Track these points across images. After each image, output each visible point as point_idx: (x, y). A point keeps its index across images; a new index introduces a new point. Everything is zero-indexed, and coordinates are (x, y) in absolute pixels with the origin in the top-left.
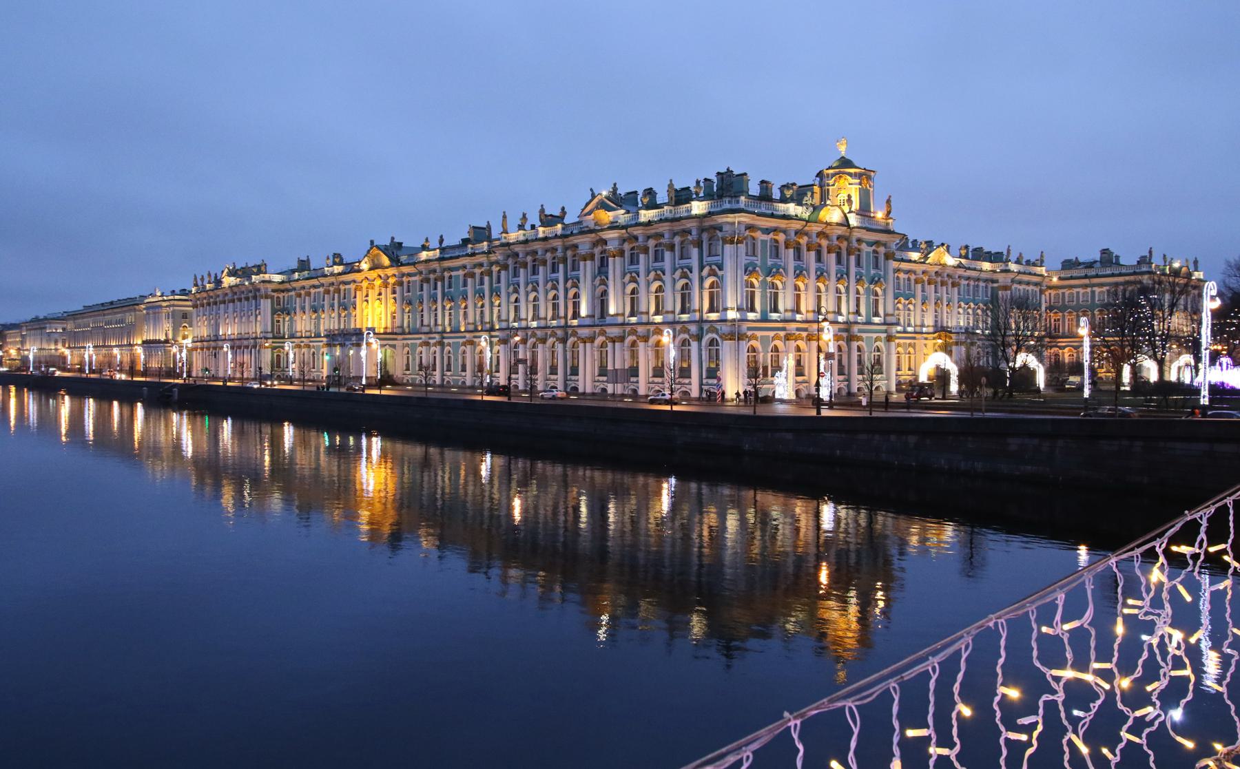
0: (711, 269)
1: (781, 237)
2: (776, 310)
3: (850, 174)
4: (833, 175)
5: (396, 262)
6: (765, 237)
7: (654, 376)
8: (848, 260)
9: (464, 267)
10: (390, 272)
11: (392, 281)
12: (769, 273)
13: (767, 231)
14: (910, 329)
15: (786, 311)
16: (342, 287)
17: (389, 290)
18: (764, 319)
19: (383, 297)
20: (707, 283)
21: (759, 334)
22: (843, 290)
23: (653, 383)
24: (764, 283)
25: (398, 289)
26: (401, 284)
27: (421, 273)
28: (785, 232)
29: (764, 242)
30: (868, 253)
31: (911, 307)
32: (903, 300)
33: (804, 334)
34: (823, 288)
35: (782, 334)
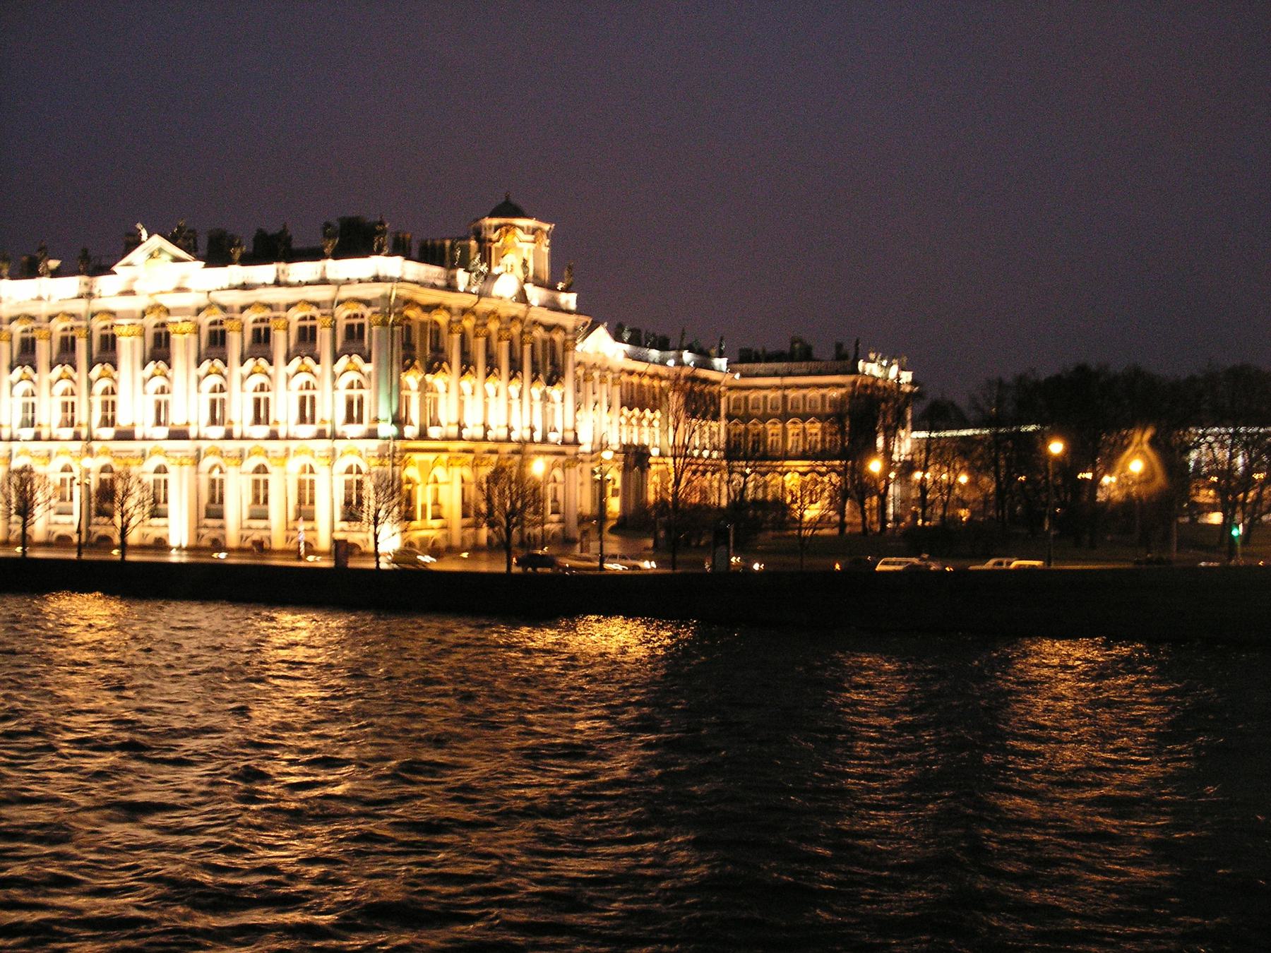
0: (351, 361)
1: (442, 318)
2: (436, 423)
3: (522, 228)
4: (497, 228)
6: (425, 317)
7: (251, 518)
8: (522, 351)
12: (430, 370)
13: (428, 308)
15: (449, 424)
18: (423, 436)
20: (343, 382)
21: (417, 457)
22: (515, 394)
23: (250, 528)
24: (424, 387)
28: (448, 309)
29: (423, 324)
30: (544, 342)
33: (470, 457)
34: (491, 393)
35: (444, 456)
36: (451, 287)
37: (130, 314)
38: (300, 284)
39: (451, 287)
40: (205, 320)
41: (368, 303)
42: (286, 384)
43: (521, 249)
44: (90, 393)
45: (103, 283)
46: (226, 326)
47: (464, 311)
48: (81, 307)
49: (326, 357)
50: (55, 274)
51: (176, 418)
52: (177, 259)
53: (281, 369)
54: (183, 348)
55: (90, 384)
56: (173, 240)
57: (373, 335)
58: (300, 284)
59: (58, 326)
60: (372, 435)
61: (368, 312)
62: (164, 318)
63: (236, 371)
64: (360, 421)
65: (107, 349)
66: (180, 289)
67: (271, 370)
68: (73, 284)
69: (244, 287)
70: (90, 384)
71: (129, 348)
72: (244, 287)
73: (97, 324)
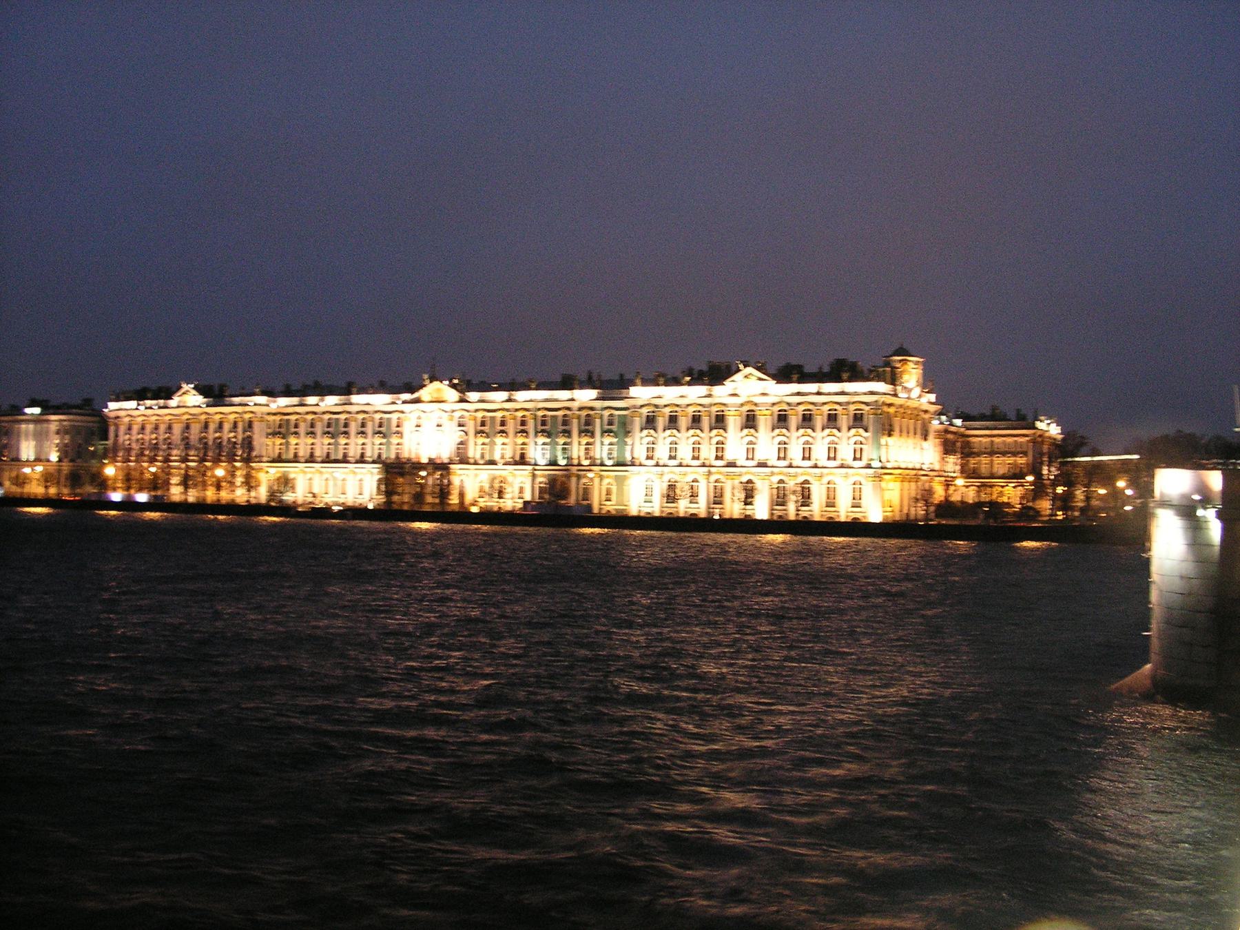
11: (457, 414)
36: (895, 395)
37: (734, 405)
38: (829, 394)
39: (895, 395)
40: (776, 408)
41: (867, 404)
42: (821, 441)
43: (912, 374)
45: (717, 390)
46: (789, 412)
47: (901, 406)
48: (706, 401)
49: (844, 428)
50: (689, 384)
51: (760, 456)
52: (760, 379)
53: (819, 434)
54: (764, 422)
56: (758, 369)
57: (870, 420)
58: (829, 394)
59: (691, 410)
60: (869, 466)
61: (867, 408)
62: (753, 408)
63: (794, 434)
64: (860, 459)
65: (720, 421)
66: (764, 394)
67: (813, 434)
68: (701, 390)
69: (798, 394)
71: (733, 422)
72: (798, 394)
73: (714, 409)
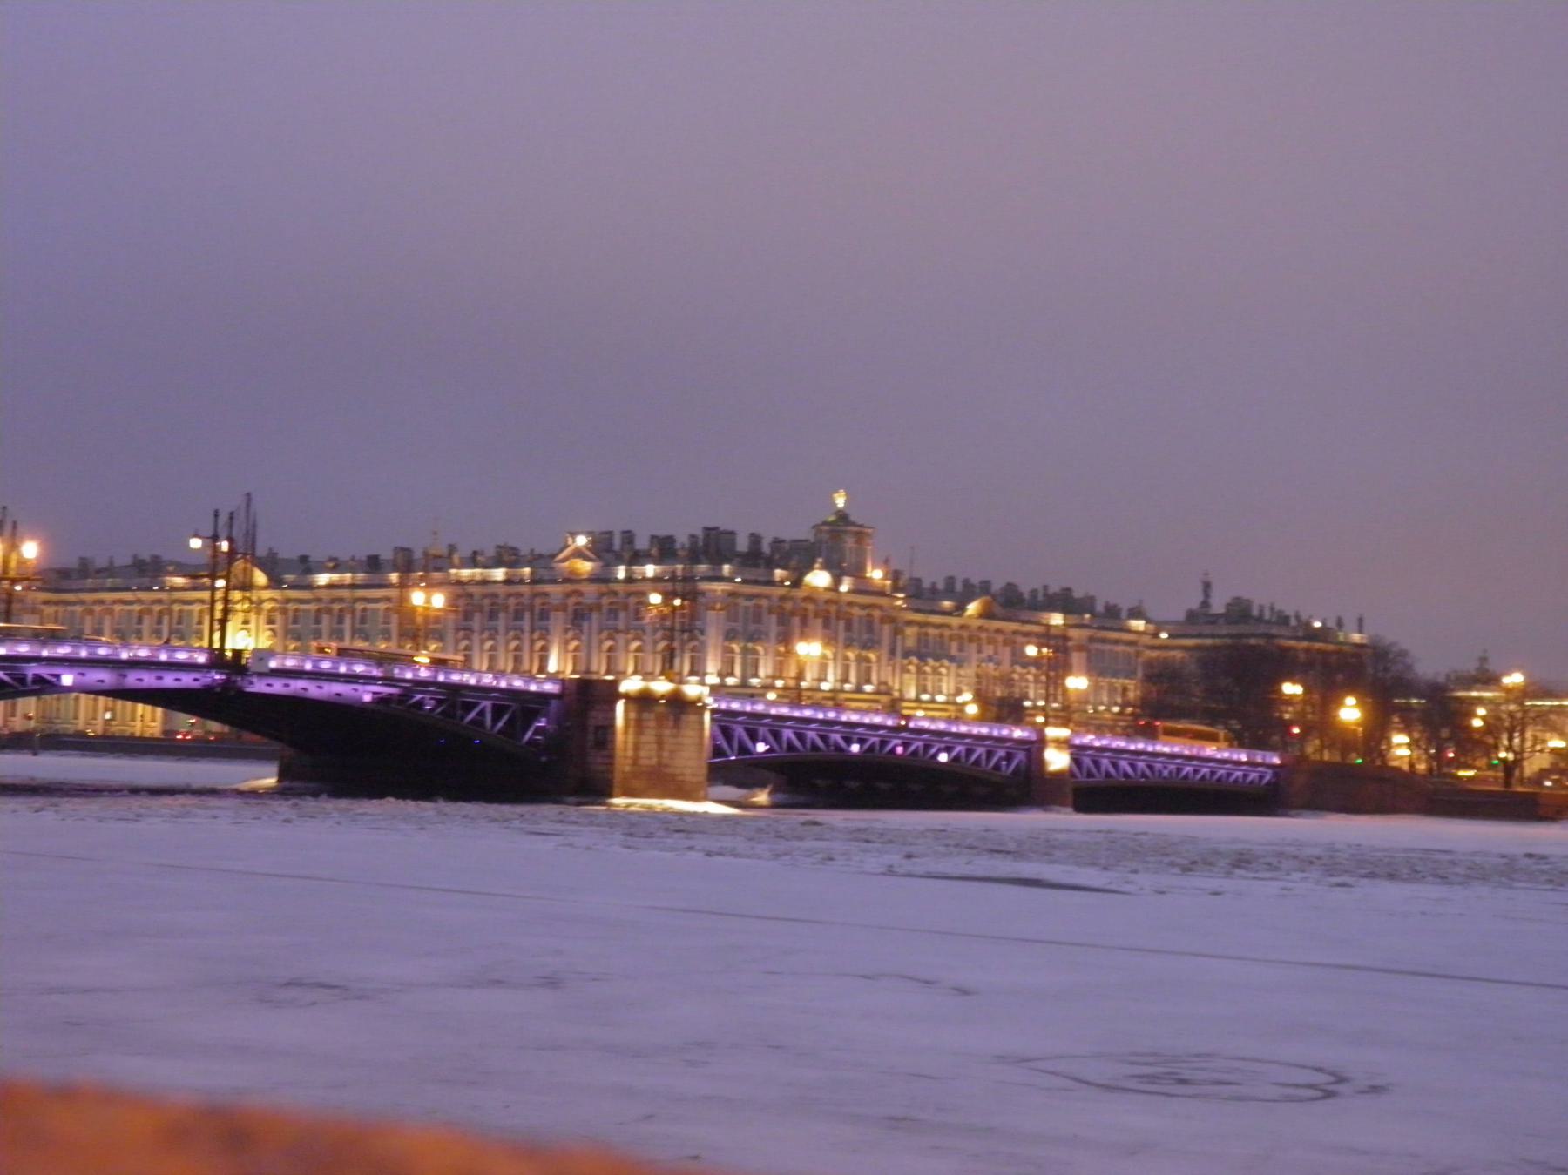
5: (275, 582)
9: (388, 599)
10: (267, 594)
11: (267, 606)
14: (940, 698)
16: (176, 607)
17: (263, 619)
19: (252, 626)
24: (745, 651)
25: (278, 617)
26: (284, 612)
27: (319, 600)
28: (768, 597)
29: (747, 608)
31: (943, 670)
32: (931, 661)
44: (532, 650)
55: (532, 642)
70: (532, 642)
